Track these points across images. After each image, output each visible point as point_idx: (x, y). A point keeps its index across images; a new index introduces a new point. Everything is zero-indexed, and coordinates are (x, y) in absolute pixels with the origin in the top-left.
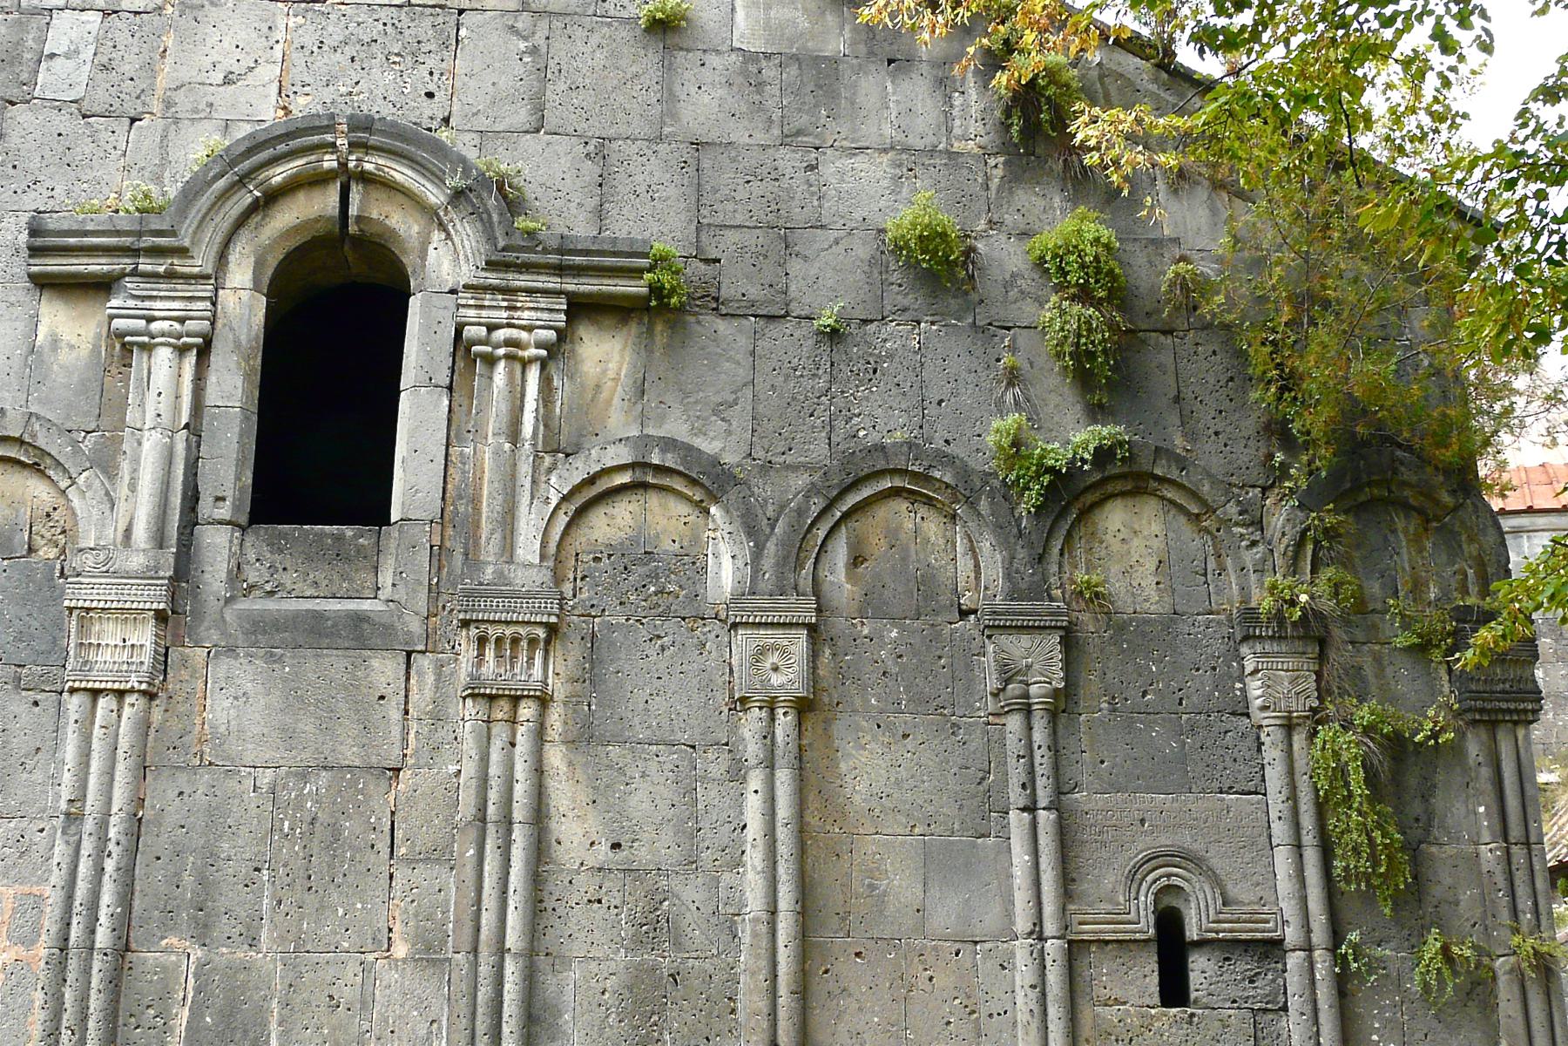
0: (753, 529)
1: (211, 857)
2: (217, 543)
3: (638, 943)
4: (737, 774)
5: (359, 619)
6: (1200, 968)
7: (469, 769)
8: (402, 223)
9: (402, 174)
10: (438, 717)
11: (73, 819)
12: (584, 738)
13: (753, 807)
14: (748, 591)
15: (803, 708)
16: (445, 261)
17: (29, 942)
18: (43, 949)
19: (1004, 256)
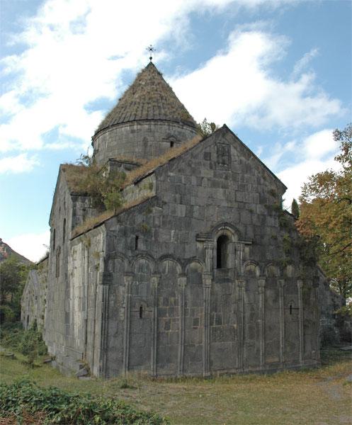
0: (261, 270)
1: (216, 304)
2: (215, 270)
3: (251, 310)
4: (259, 294)
5: (228, 279)
6: (293, 310)
7: (237, 295)
8: (229, 234)
9: (230, 229)
10: (235, 288)
11: (205, 301)
12: (246, 290)
13: (261, 297)
14: (260, 276)
15: (265, 287)
16: (234, 239)
17: (202, 312)
18: (204, 313)
19: (280, 239)
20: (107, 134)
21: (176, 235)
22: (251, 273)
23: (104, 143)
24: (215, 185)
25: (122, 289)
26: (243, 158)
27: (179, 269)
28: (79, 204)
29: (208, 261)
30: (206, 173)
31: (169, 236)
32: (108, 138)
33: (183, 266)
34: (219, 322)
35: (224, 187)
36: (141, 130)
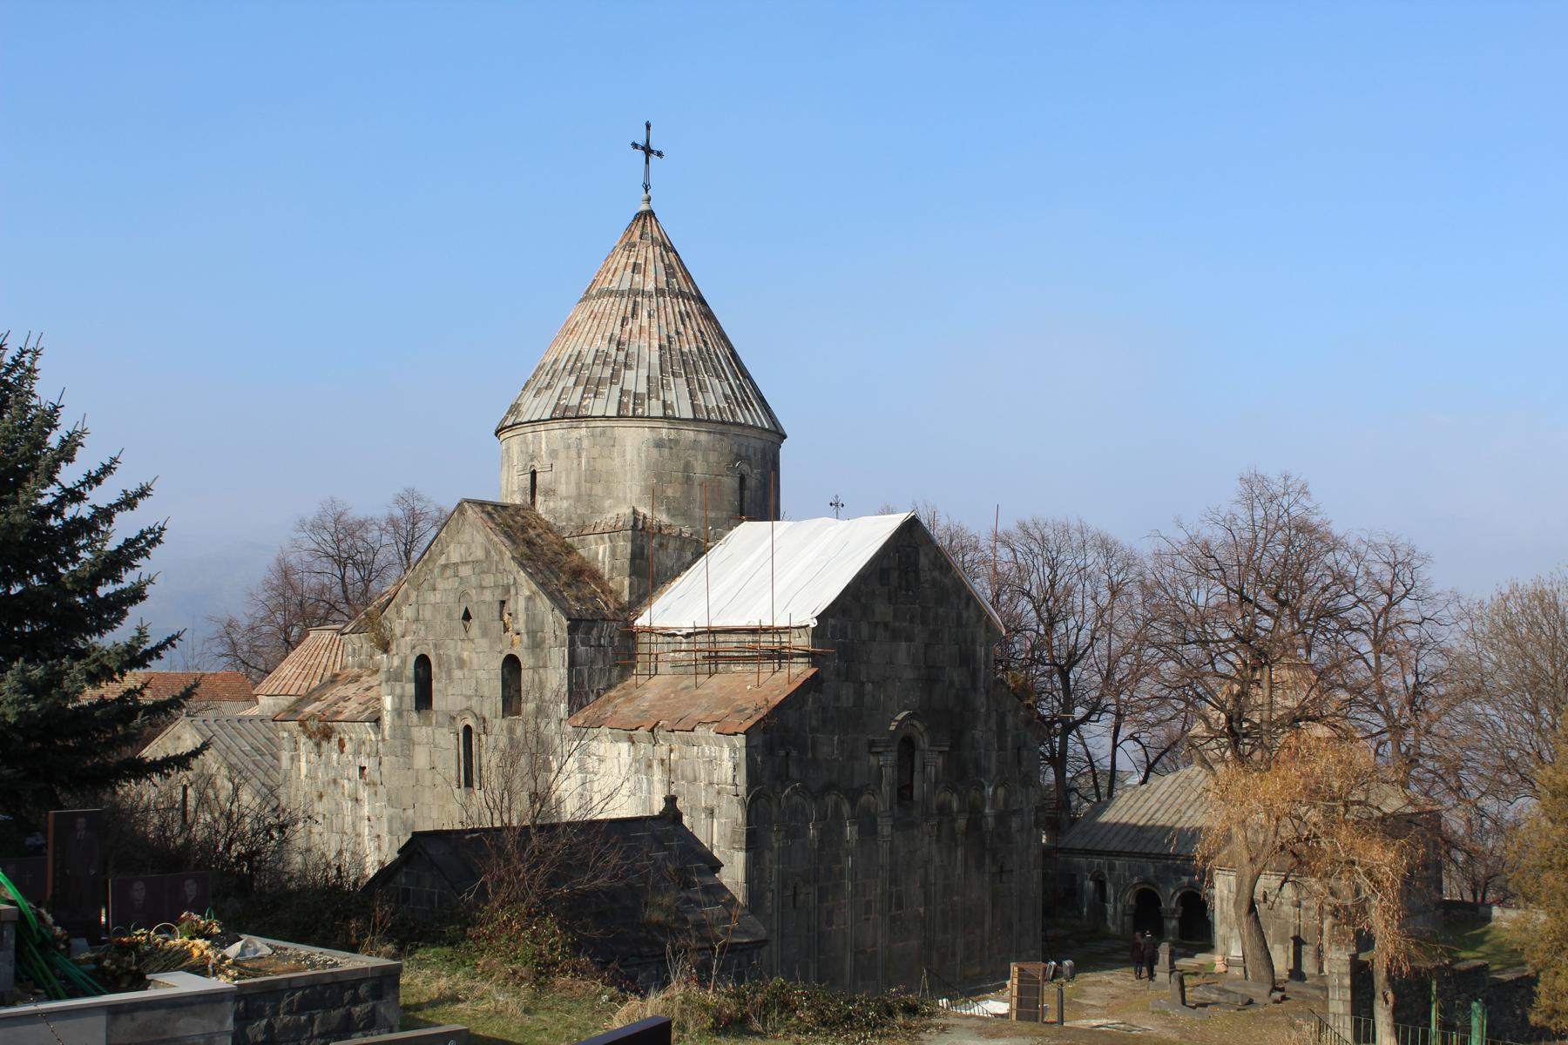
8: (916, 734)
12: (938, 841)
20: (583, 432)
21: (841, 742)
22: (944, 809)
23: (573, 453)
24: (895, 635)
25: (768, 855)
26: (936, 574)
27: (846, 809)
28: (579, 637)
29: (885, 788)
30: (882, 610)
31: (829, 747)
32: (586, 443)
33: (853, 804)
34: (899, 906)
35: (909, 639)
36: (676, 442)
